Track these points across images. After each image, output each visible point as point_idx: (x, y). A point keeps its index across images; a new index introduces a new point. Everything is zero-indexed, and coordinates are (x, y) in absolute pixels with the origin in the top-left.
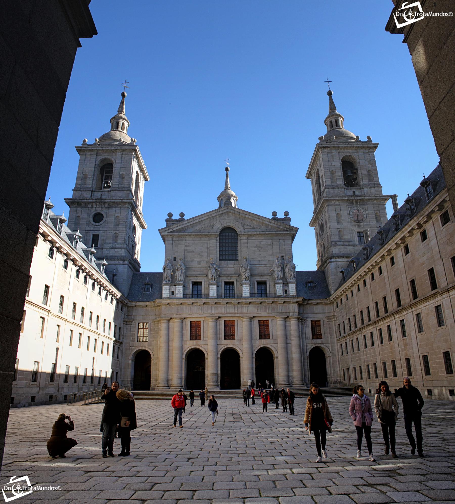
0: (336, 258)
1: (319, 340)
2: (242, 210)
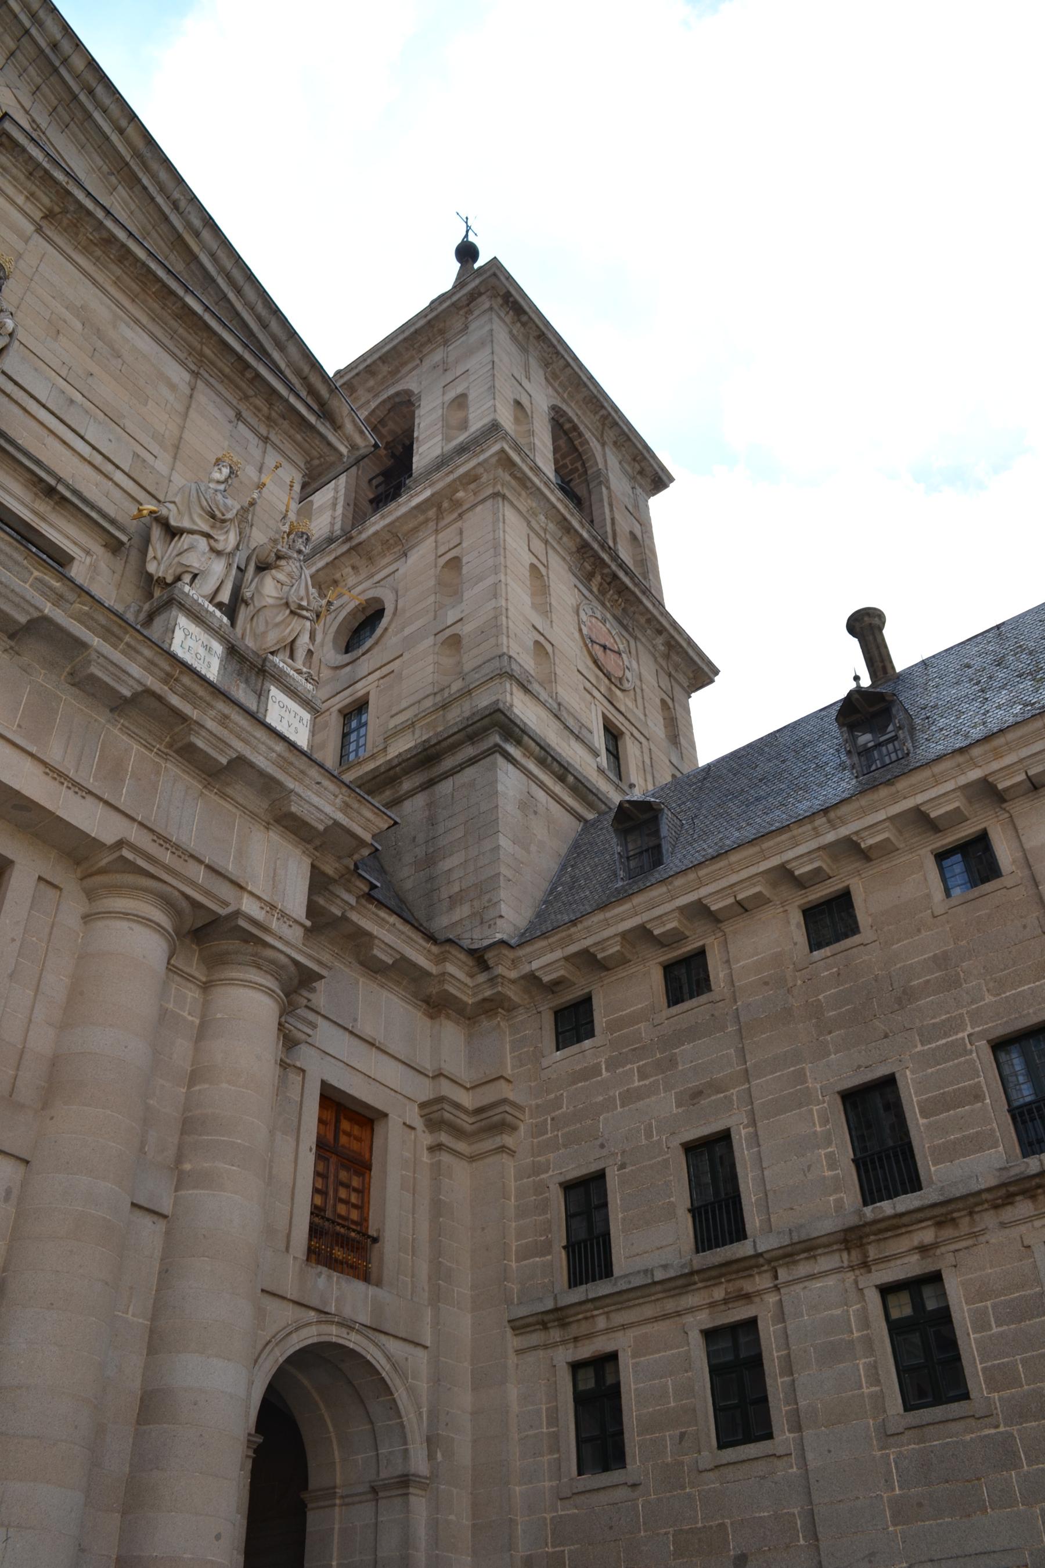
0: (529, 753)
1: (358, 1287)
2: (92, 65)
